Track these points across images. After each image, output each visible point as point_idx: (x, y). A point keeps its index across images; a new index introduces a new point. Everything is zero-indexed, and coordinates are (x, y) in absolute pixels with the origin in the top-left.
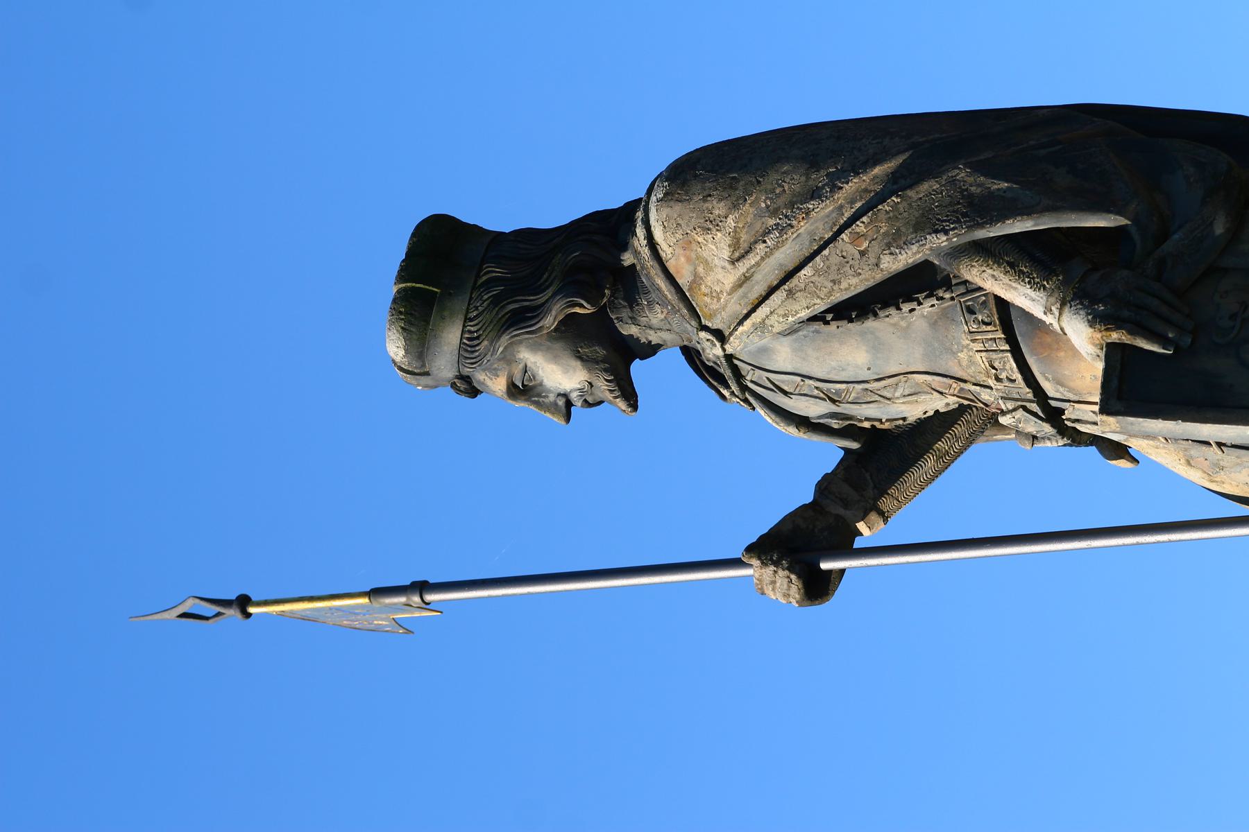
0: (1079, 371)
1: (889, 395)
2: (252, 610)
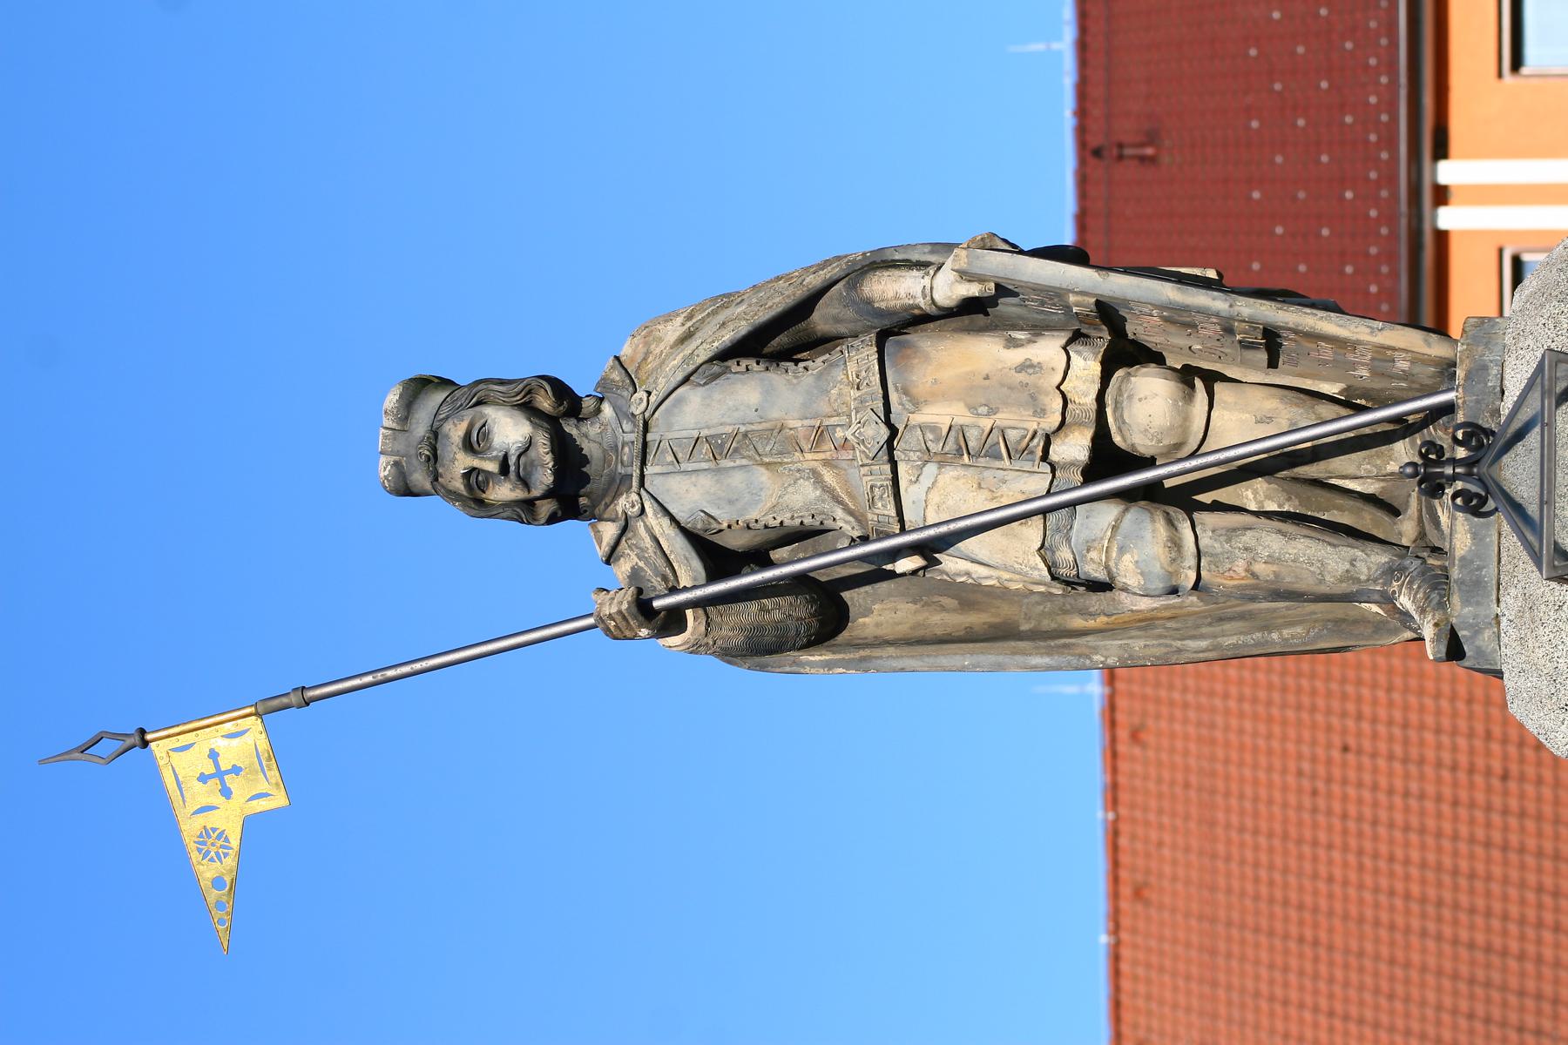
0: (924, 376)
1: (760, 451)
2: (149, 737)
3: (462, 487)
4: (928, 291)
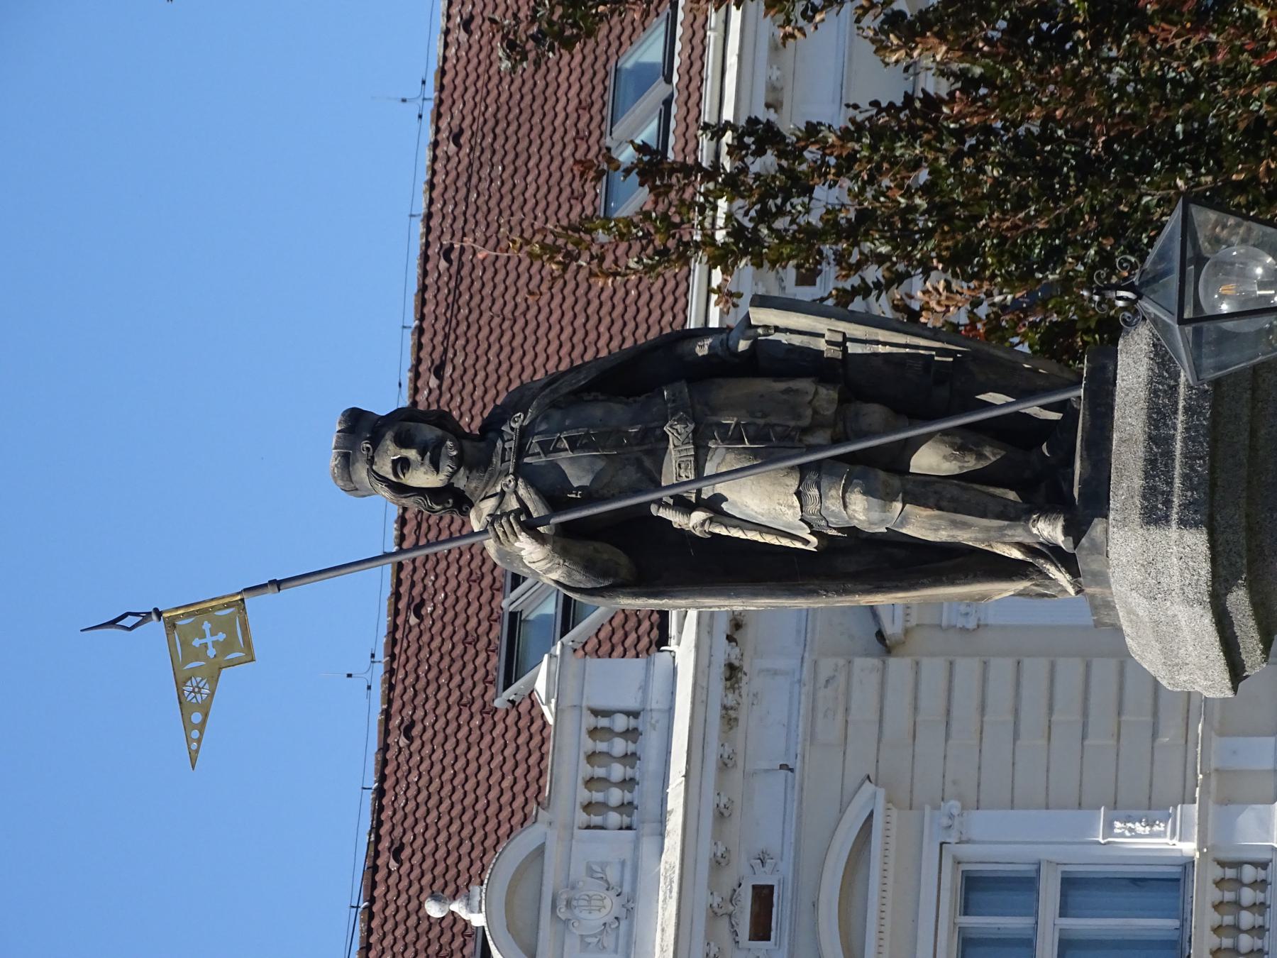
3: (390, 471)
4: (725, 342)
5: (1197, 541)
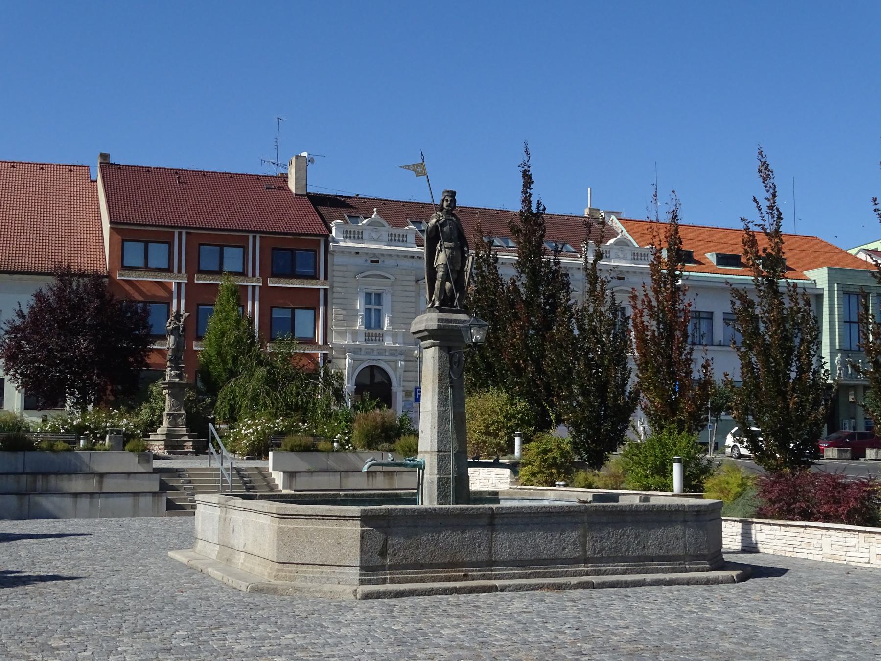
5: (435, 327)
